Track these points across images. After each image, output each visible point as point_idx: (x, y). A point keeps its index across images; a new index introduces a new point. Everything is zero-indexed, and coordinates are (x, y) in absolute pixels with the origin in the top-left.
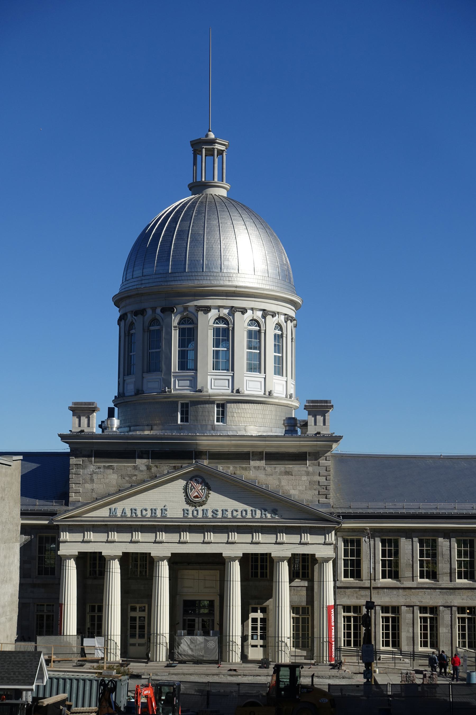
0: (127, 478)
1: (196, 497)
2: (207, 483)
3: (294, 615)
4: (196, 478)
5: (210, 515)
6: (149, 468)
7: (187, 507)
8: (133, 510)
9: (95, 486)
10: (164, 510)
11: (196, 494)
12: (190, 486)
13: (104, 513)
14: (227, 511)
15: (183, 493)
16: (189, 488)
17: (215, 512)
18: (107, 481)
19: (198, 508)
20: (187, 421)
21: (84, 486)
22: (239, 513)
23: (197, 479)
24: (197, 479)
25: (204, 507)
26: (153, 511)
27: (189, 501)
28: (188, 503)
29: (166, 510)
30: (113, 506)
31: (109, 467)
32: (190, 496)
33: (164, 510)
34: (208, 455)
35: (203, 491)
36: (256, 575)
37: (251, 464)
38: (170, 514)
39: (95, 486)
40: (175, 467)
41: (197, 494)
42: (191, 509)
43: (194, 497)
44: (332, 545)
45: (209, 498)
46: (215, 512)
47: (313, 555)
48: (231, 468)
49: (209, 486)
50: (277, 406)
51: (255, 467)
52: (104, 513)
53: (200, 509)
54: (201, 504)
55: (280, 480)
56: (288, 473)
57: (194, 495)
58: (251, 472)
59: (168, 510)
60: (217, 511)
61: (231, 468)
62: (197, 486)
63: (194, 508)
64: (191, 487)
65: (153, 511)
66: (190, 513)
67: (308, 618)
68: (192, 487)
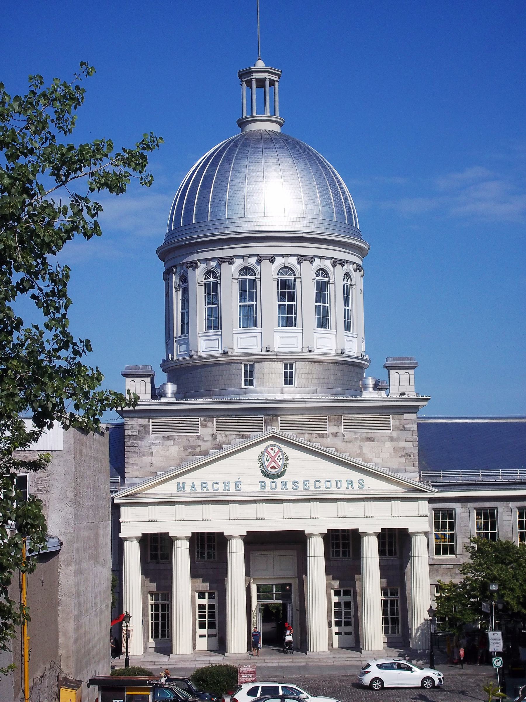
0: (189, 450)
1: (273, 468)
2: (284, 452)
3: (383, 598)
5: (290, 486)
6: (214, 438)
7: (265, 479)
8: (204, 484)
9: (153, 459)
11: (273, 464)
12: (266, 456)
14: (308, 482)
17: (296, 483)
18: (167, 453)
19: (275, 480)
20: (252, 383)
21: (142, 460)
22: (322, 485)
23: (273, 448)
24: (273, 448)
25: (282, 479)
29: (240, 483)
30: (180, 480)
31: (168, 438)
33: (238, 483)
34: (279, 421)
36: (337, 552)
37: (328, 430)
39: (153, 459)
40: (243, 435)
42: (268, 481)
43: (271, 468)
46: (295, 483)
47: (406, 530)
48: (306, 436)
50: (335, 364)
51: (332, 434)
53: (278, 480)
55: (361, 447)
56: (370, 439)
57: (271, 466)
58: (329, 439)
60: (297, 482)
61: (306, 436)
62: (273, 456)
63: (271, 480)
65: (227, 485)
66: (268, 485)
67: (397, 600)
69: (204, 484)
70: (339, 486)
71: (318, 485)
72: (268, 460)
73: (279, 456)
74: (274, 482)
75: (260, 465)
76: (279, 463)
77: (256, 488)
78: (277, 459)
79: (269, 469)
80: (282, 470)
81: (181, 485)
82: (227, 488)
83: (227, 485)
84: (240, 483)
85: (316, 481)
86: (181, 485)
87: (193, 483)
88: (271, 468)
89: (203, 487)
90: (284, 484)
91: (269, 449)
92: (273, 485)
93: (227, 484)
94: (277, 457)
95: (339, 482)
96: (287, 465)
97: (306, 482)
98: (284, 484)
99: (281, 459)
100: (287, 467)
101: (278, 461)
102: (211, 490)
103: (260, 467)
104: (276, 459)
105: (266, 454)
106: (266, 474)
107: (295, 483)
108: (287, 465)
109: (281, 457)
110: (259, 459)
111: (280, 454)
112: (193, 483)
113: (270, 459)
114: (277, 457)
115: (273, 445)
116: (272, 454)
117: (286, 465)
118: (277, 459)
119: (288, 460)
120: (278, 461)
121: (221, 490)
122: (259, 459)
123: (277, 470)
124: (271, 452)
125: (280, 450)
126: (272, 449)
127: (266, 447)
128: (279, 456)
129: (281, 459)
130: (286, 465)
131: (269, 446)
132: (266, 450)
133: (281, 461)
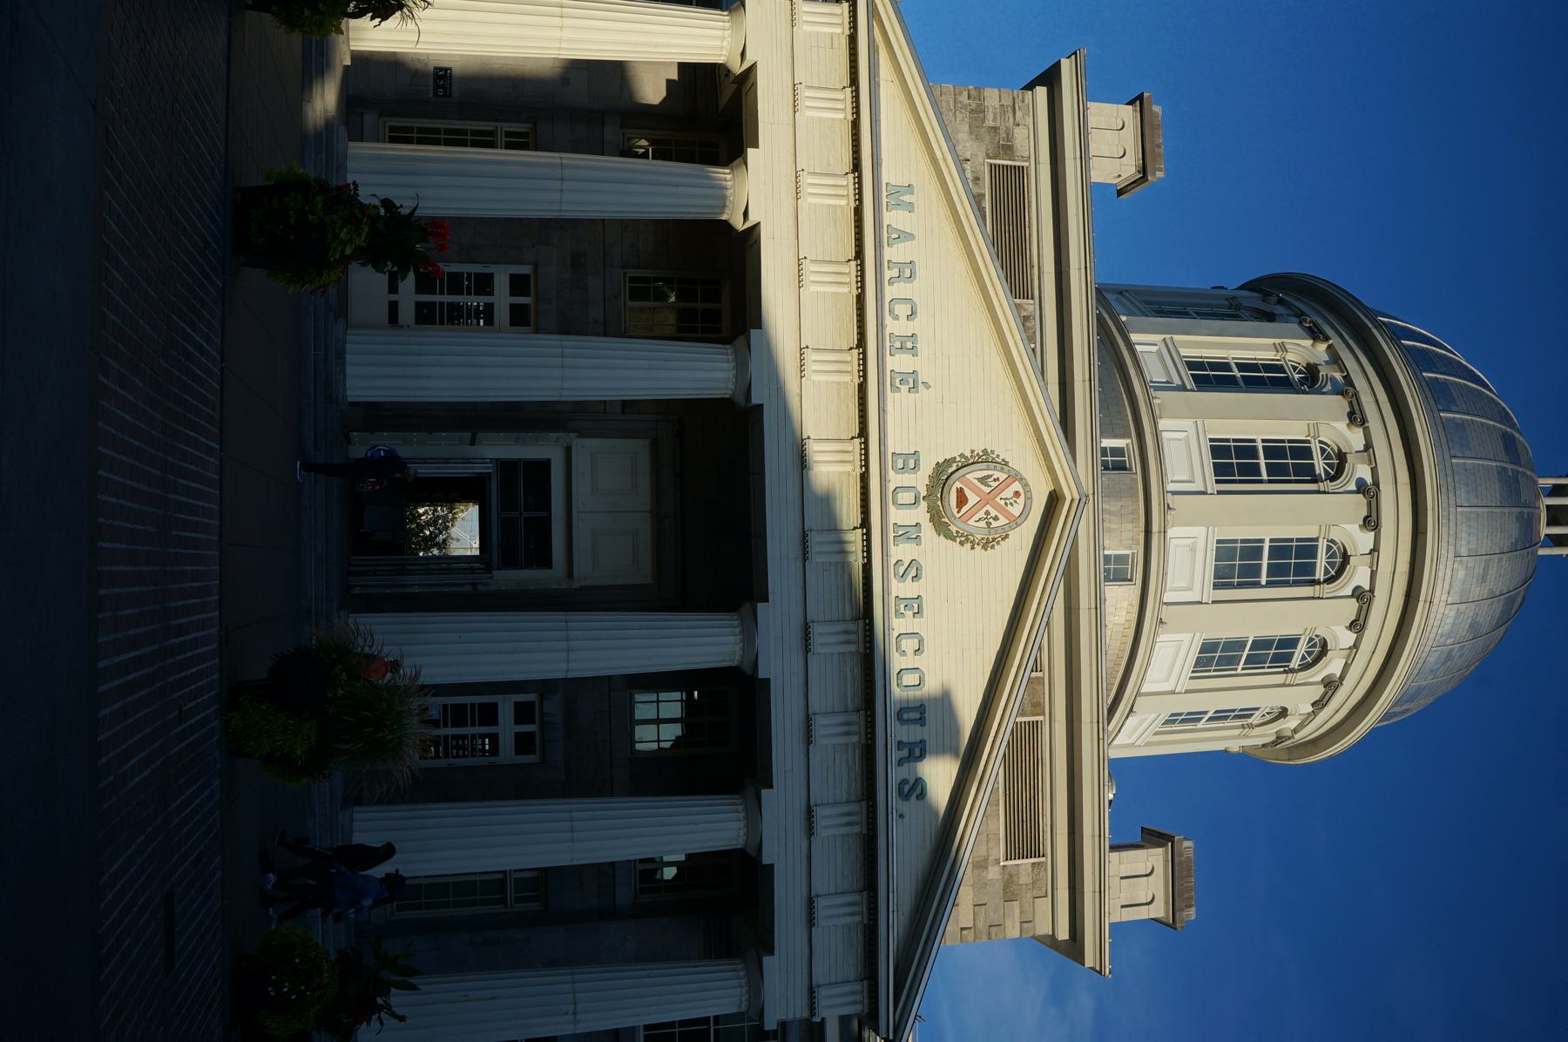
1: (962, 499)
2: (1007, 536)
4: (1022, 497)
7: (927, 468)
8: (908, 271)
10: (913, 382)
11: (972, 499)
12: (997, 474)
14: (918, 613)
15: (972, 451)
17: (913, 573)
19: (924, 505)
23: (1021, 500)
24: (1021, 500)
25: (928, 529)
26: (909, 345)
28: (940, 468)
29: (914, 388)
32: (964, 475)
33: (913, 382)
42: (921, 480)
43: (960, 492)
45: (957, 545)
49: (998, 543)
53: (921, 514)
54: (939, 522)
57: (967, 492)
62: (998, 499)
63: (924, 493)
64: (995, 480)
66: (906, 479)
68: (995, 484)
69: (908, 271)
70: (905, 716)
72: (983, 480)
73: (996, 518)
75: (969, 455)
76: (976, 517)
77: (896, 443)
78: (987, 513)
79: (958, 485)
80: (953, 528)
81: (907, 198)
82: (898, 345)
83: (909, 345)
84: (915, 387)
85: (921, 642)
86: (907, 198)
87: (910, 237)
88: (960, 492)
89: (900, 265)
90: (910, 534)
91: (1017, 486)
93: (909, 345)
94: (993, 513)
95: (917, 716)
97: (916, 606)
98: (910, 534)
99: (989, 524)
100: (962, 543)
101: (981, 514)
102: (890, 292)
103: (962, 456)
104: (988, 507)
105: (1003, 476)
106: (942, 476)
107: (914, 570)
108: (969, 545)
109: (995, 524)
110: (985, 451)
111: (1003, 521)
112: (910, 237)
113: (987, 490)
114: (993, 513)
115: (1029, 499)
116: (1002, 495)
117: (967, 540)
118: (987, 513)
119: (985, 547)
120: (981, 514)
121: (891, 326)
122: (985, 451)
124: (1009, 493)
125: (1015, 522)
126: (1017, 494)
127: (1021, 480)
128: (996, 518)
129: (989, 524)
130: (967, 540)
131: (1025, 485)
132: (1015, 476)
133: (983, 524)
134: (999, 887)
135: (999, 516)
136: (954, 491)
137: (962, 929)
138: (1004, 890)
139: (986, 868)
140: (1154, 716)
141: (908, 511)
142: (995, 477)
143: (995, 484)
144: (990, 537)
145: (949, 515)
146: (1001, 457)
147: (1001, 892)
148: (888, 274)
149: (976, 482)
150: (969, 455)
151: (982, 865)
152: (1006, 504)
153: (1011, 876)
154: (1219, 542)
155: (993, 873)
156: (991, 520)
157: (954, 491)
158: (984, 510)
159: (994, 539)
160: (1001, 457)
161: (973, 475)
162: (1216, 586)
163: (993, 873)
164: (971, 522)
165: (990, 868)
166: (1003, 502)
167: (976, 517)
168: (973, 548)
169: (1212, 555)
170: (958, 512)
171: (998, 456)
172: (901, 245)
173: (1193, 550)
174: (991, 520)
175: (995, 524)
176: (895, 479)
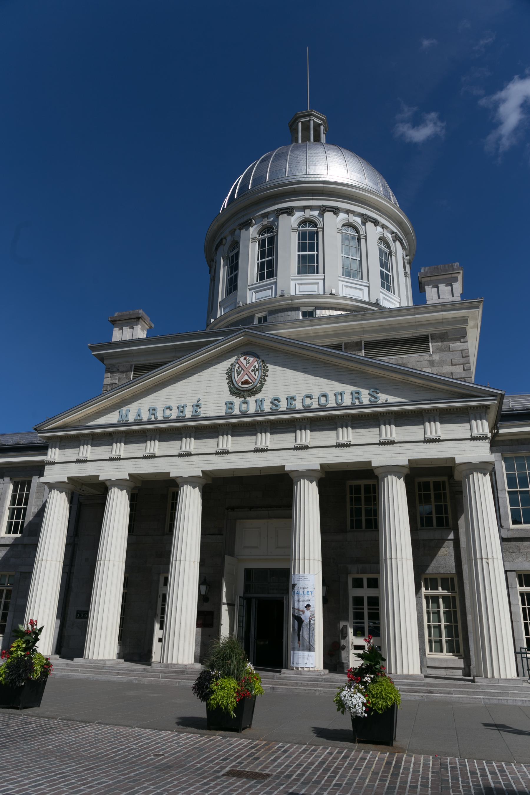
1: (246, 382)
7: (233, 398)
11: (246, 377)
12: (236, 368)
13: (112, 418)
15: (227, 379)
16: (234, 372)
19: (248, 399)
25: (258, 396)
26: (182, 408)
27: (235, 391)
28: (232, 393)
32: (236, 382)
35: (257, 373)
38: (204, 412)
41: (247, 378)
42: (237, 401)
44: (487, 441)
45: (266, 383)
52: (112, 418)
53: (251, 400)
54: (253, 392)
57: (243, 380)
59: (202, 406)
60: (277, 400)
62: (247, 367)
64: (239, 369)
68: (240, 369)
70: (340, 401)
71: (308, 402)
72: (239, 373)
73: (255, 367)
74: (246, 402)
75: (228, 380)
76: (254, 375)
78: (252, 371)
79: (240, 384)
87: (139, 410)
88: (242, 383)
92: (244, 406)
96: (266, 378)
99: (257, 370)
102: (160, 418)
104: (250, 371)
105: (237, 365)
108: (266, 378)
109: (257, 367)
112: (139, 410)
116: (245, 365)
123: (251, 385)
128: (255, 367)
129: (257, 370)
130: (264, 378)
134: (442, 354)
135: (254, 365)
136: (242, 386)
137: (464, 370)
138: (444, 351)
139: (434, 361)
140: (381, 294)
141: (250, 405)
142: (237, 369)
143: (240, 369)
144: (263, 368)
145: (252, 387)
146: (230, 366)
147: (445, 353)
148: (153, 419)
149: (239, 377)
150: (228, 380)
151: (432, 364)
152: (249, 363)
153: (437, 349)
154: (298, 273)
155: (436, 357)
156: (256, 369)
157: (242, 386)
158: (251, 372)
159: (264, 367)
160: (230, 366)
161: (236, 377)
162: (318, 273)
163: (436, 357)
164: (256, 377)
165: (434, 359)
166: (248, 365)
167: (254, 375)
168: (267, 376)
169: (304, 277)
170: (251, 383)
171: (229, 368)
172: (142, 414)
173: (301, 284)
174: (256, 369)
175: (257, 367)
176: (236, 411)
